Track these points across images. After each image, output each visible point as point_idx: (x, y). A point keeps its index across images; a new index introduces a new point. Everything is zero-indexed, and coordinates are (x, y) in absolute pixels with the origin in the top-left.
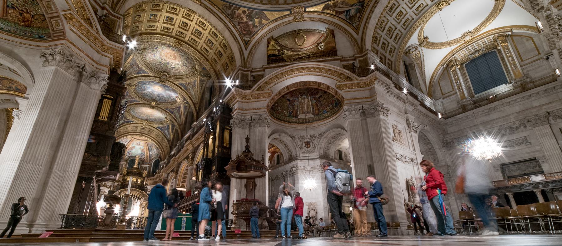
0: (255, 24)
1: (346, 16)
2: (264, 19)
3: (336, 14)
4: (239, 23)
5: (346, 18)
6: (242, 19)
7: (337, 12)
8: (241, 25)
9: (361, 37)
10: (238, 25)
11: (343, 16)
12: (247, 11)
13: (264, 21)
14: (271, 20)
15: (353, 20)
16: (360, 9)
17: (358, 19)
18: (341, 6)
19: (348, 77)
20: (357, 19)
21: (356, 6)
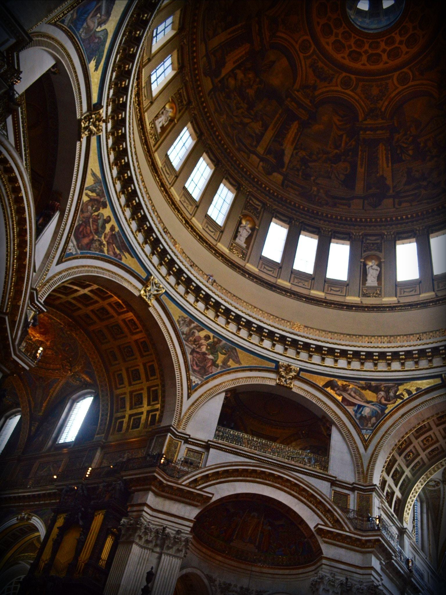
0: (216, 361)
1: (356, 412)
2: (233, 360)
3: (342, 401)
4: (193, 351)
5: (356, 416)
6: (200, 346)
7: (344, 399)
8: (195, 355)
9: (370, 455)
10: (191, 354)
11: (352, 410)
12: (212, 338)
13: (231, 363)
14: (244, 365)
15: (365, 424)
16: (378, 412)
17: (372, 426)
18: (353, 394)
19: (337, 521)
20: (370, 425)
21: (373, 405)
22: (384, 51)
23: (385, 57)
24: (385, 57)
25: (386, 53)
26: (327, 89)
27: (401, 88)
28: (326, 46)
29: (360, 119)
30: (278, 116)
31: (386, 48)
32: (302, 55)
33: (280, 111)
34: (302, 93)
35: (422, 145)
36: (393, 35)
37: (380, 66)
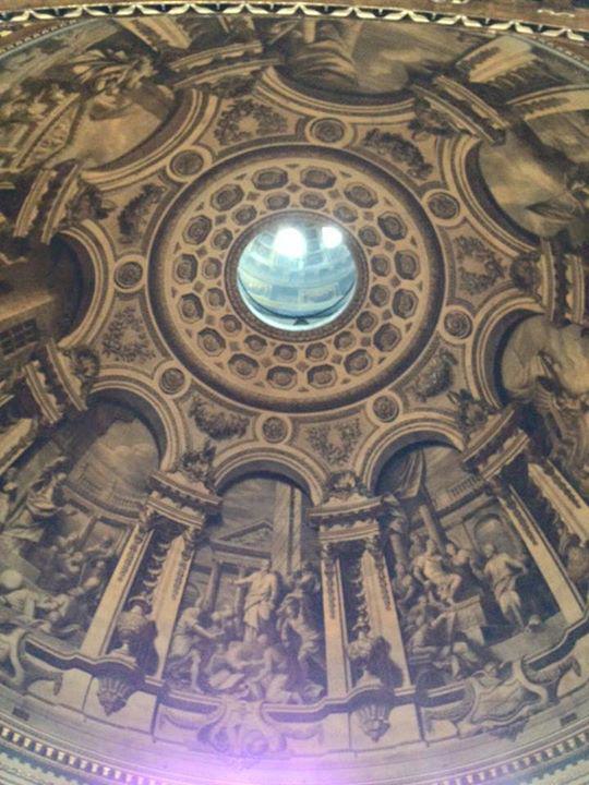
22: (253, 197)
23: (248, 187)
24: (248, 187)
25: (247, 194)
26: (379, 120)
27: (186, 146)
28: (390, 197)
29: (271, 72)
30: (539, 113)
31: (250, 203)
32: (453, 192)
33: (528, 117)
34: (455, 125)
35: (59, 95)
36: (243, 228)
37: (251, 170)
